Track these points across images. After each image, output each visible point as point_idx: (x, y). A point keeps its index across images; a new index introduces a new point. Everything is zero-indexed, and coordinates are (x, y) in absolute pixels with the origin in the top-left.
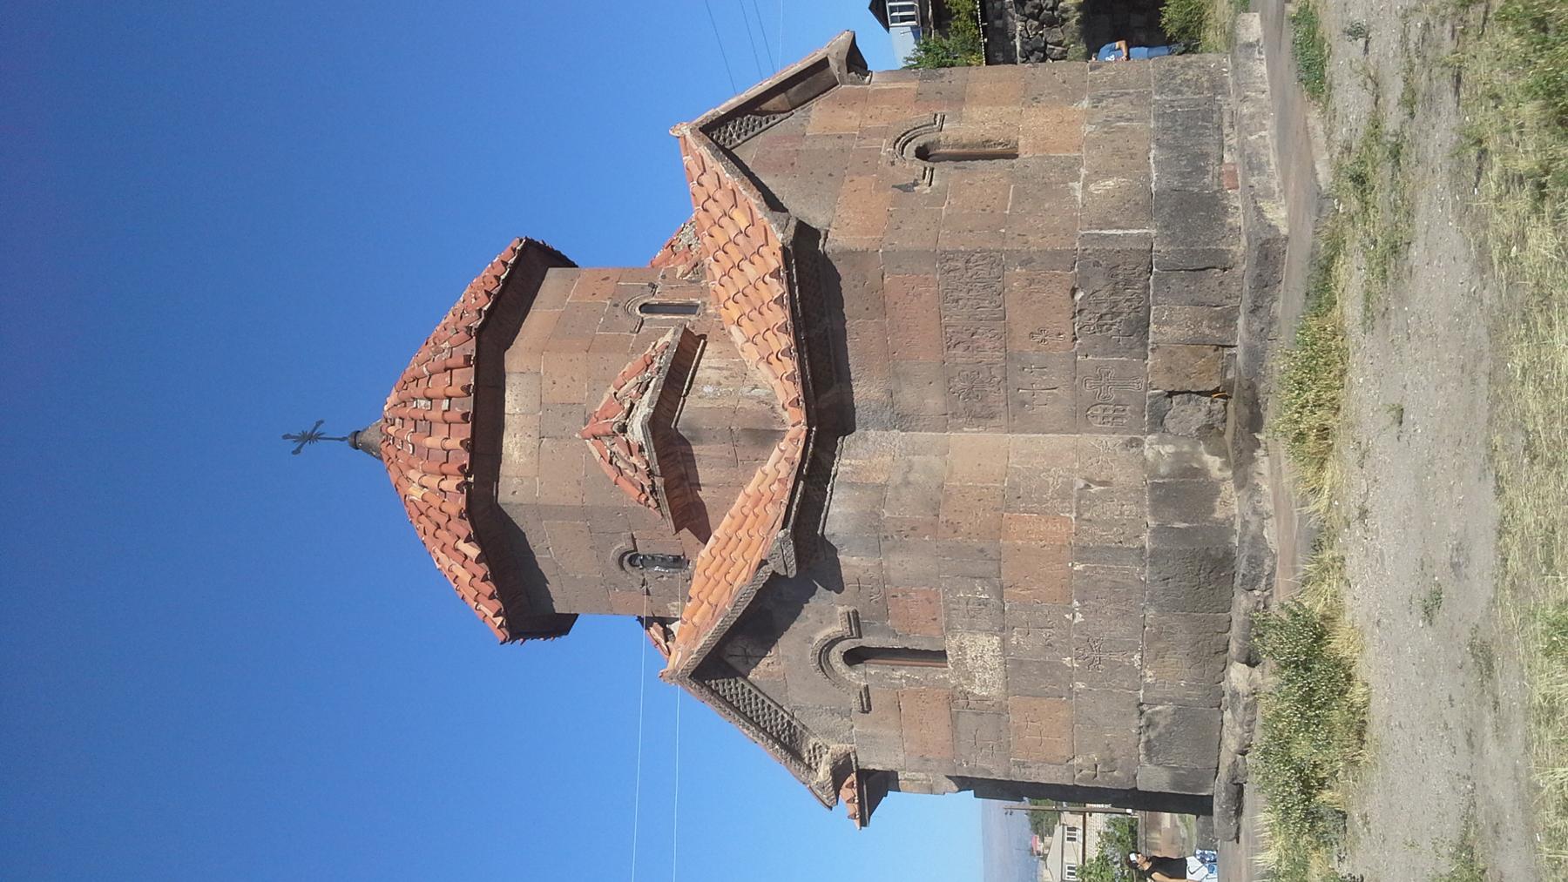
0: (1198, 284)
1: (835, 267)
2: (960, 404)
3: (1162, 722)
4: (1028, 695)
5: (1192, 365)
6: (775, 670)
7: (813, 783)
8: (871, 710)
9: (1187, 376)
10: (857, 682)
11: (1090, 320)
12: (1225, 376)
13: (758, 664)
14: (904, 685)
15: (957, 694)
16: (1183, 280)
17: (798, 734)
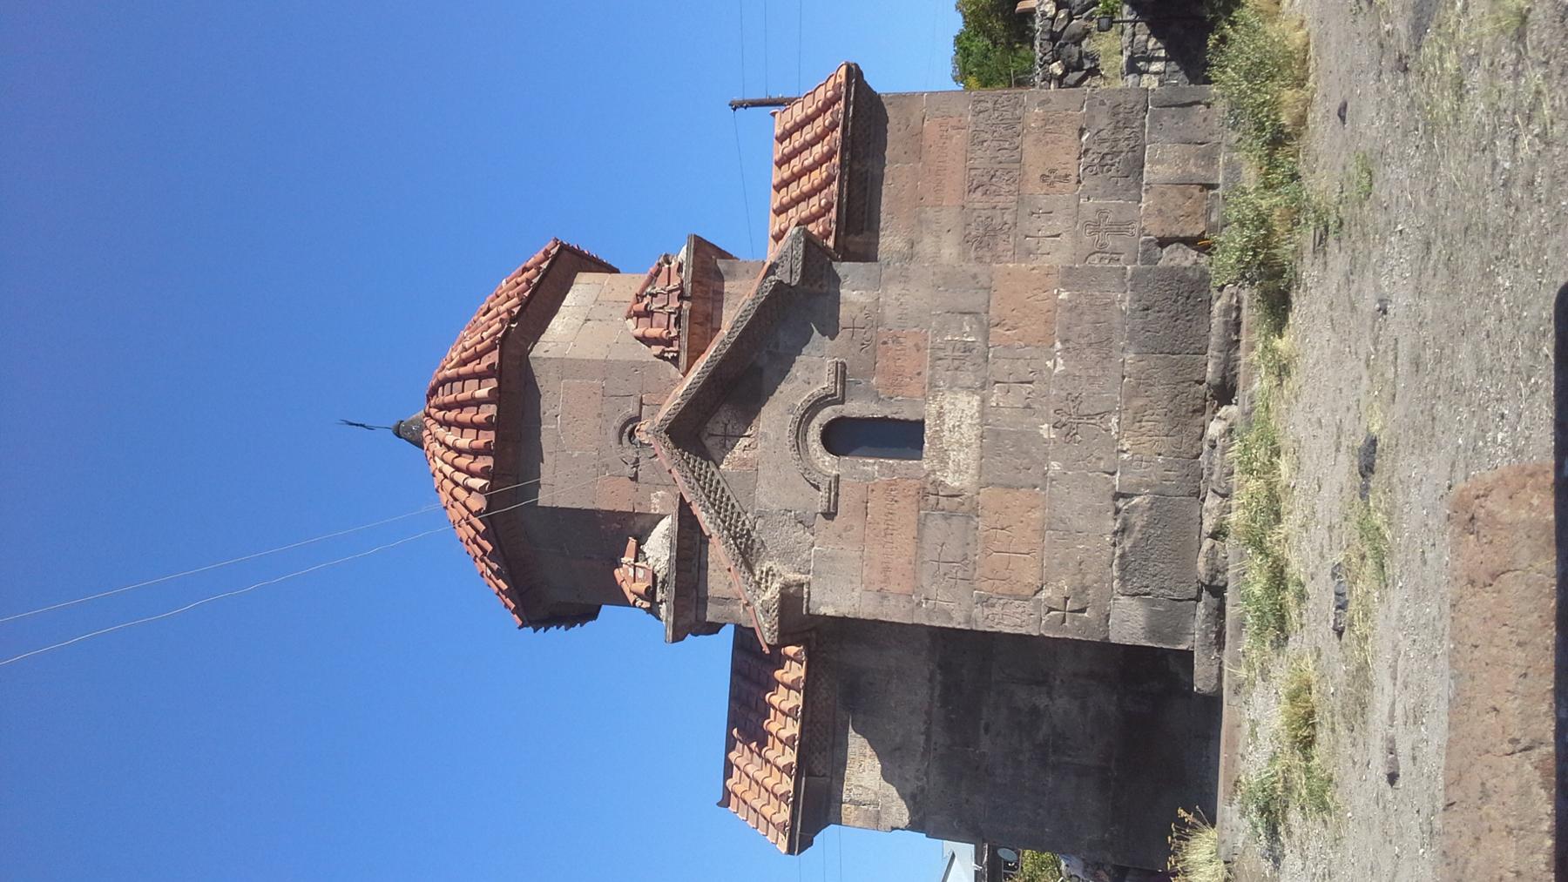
0: (1186, 122)
1: (885, 110)
2: (973, 255)
3: (1138, 521)
4: (1001, 485)
5: (1180, 206)
6: (750, 455)
7: (757, 604)
8: (836, 514)
9: (1176, 218)
10: (830, 471)
11: (1093, 160)
12: (1210, 218)
13: (733, 448)
14: (876, 475)
15: (928, 486)
16: (1173, 117)
17: (755, 550)
